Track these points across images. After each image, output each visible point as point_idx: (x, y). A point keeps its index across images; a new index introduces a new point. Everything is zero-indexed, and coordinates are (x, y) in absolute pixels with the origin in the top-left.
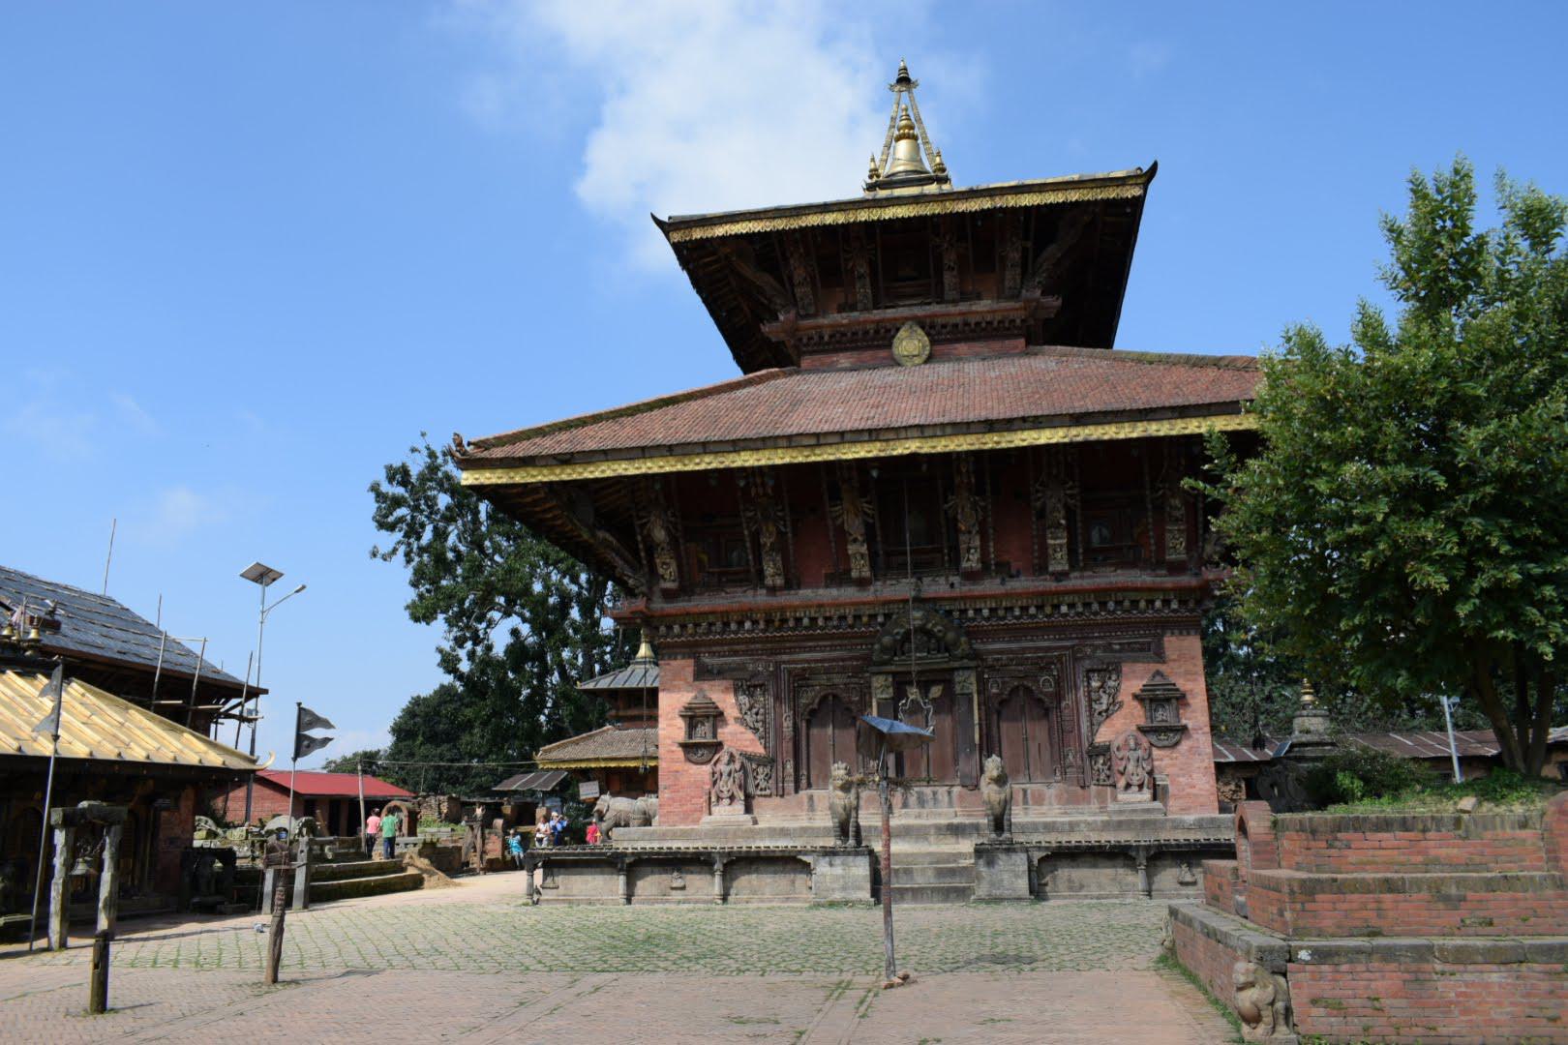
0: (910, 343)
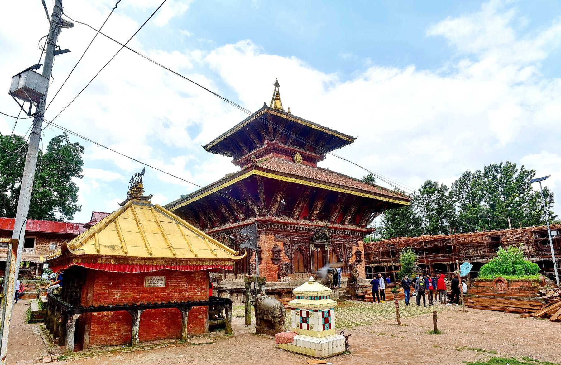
0: (298, 157)
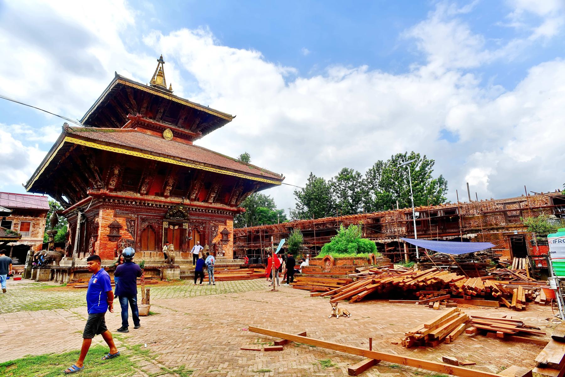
0: (168, 134)
